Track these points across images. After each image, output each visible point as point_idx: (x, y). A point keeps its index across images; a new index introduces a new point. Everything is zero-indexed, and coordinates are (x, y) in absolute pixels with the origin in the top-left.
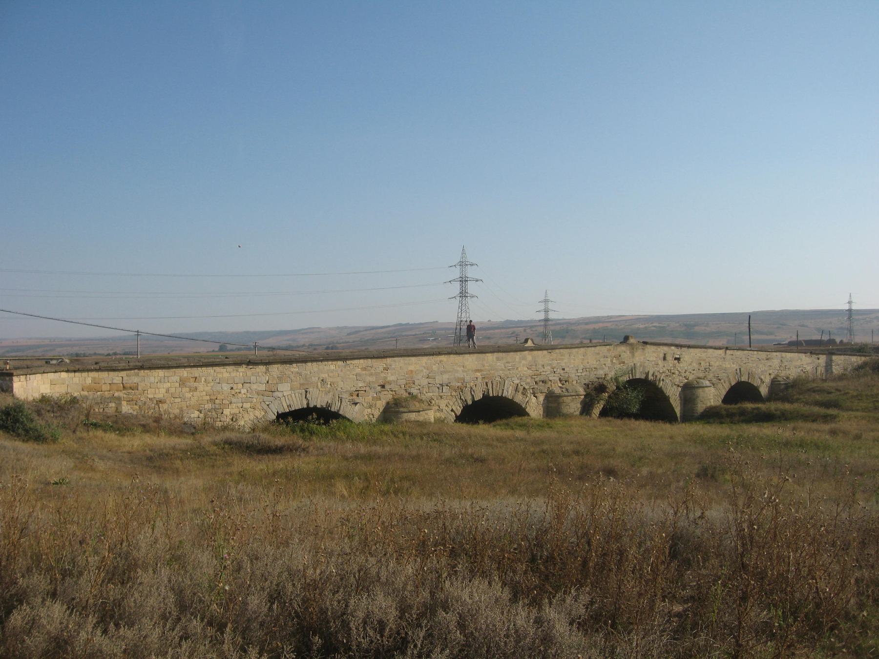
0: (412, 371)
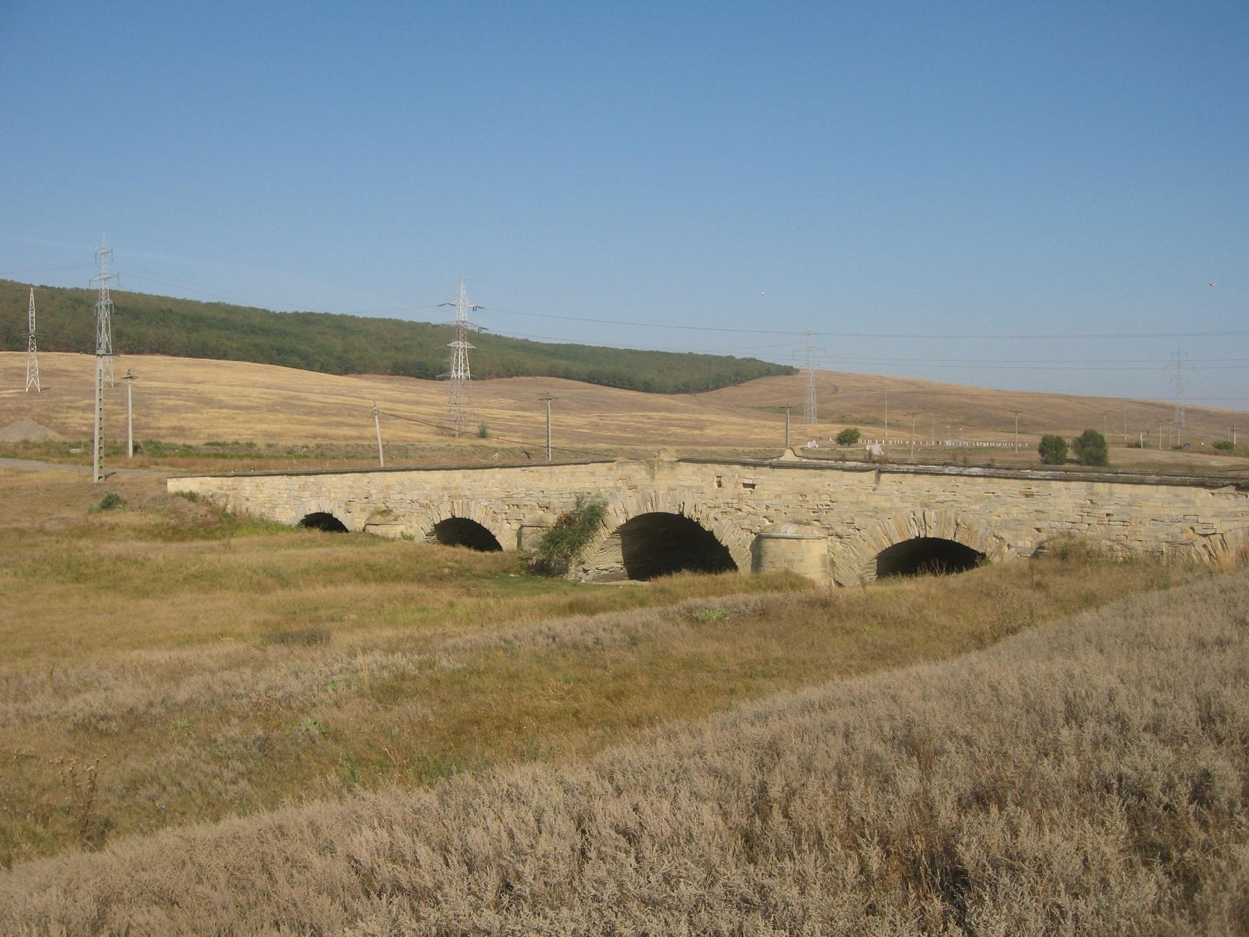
0: (387, 487)
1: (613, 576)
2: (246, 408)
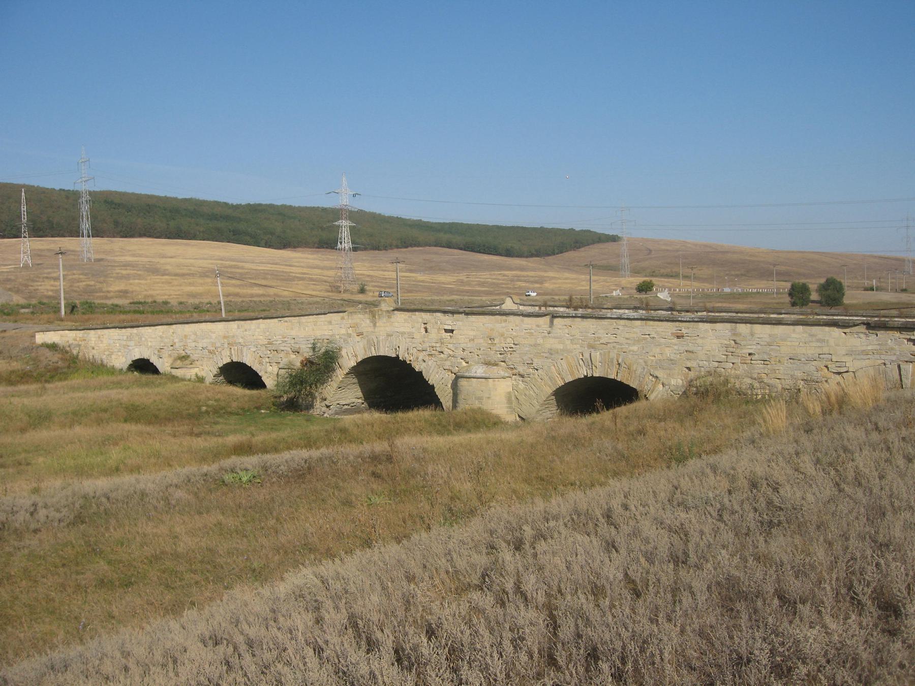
0: (186, 336)
1: (353, 410)
2: (183, 275)
